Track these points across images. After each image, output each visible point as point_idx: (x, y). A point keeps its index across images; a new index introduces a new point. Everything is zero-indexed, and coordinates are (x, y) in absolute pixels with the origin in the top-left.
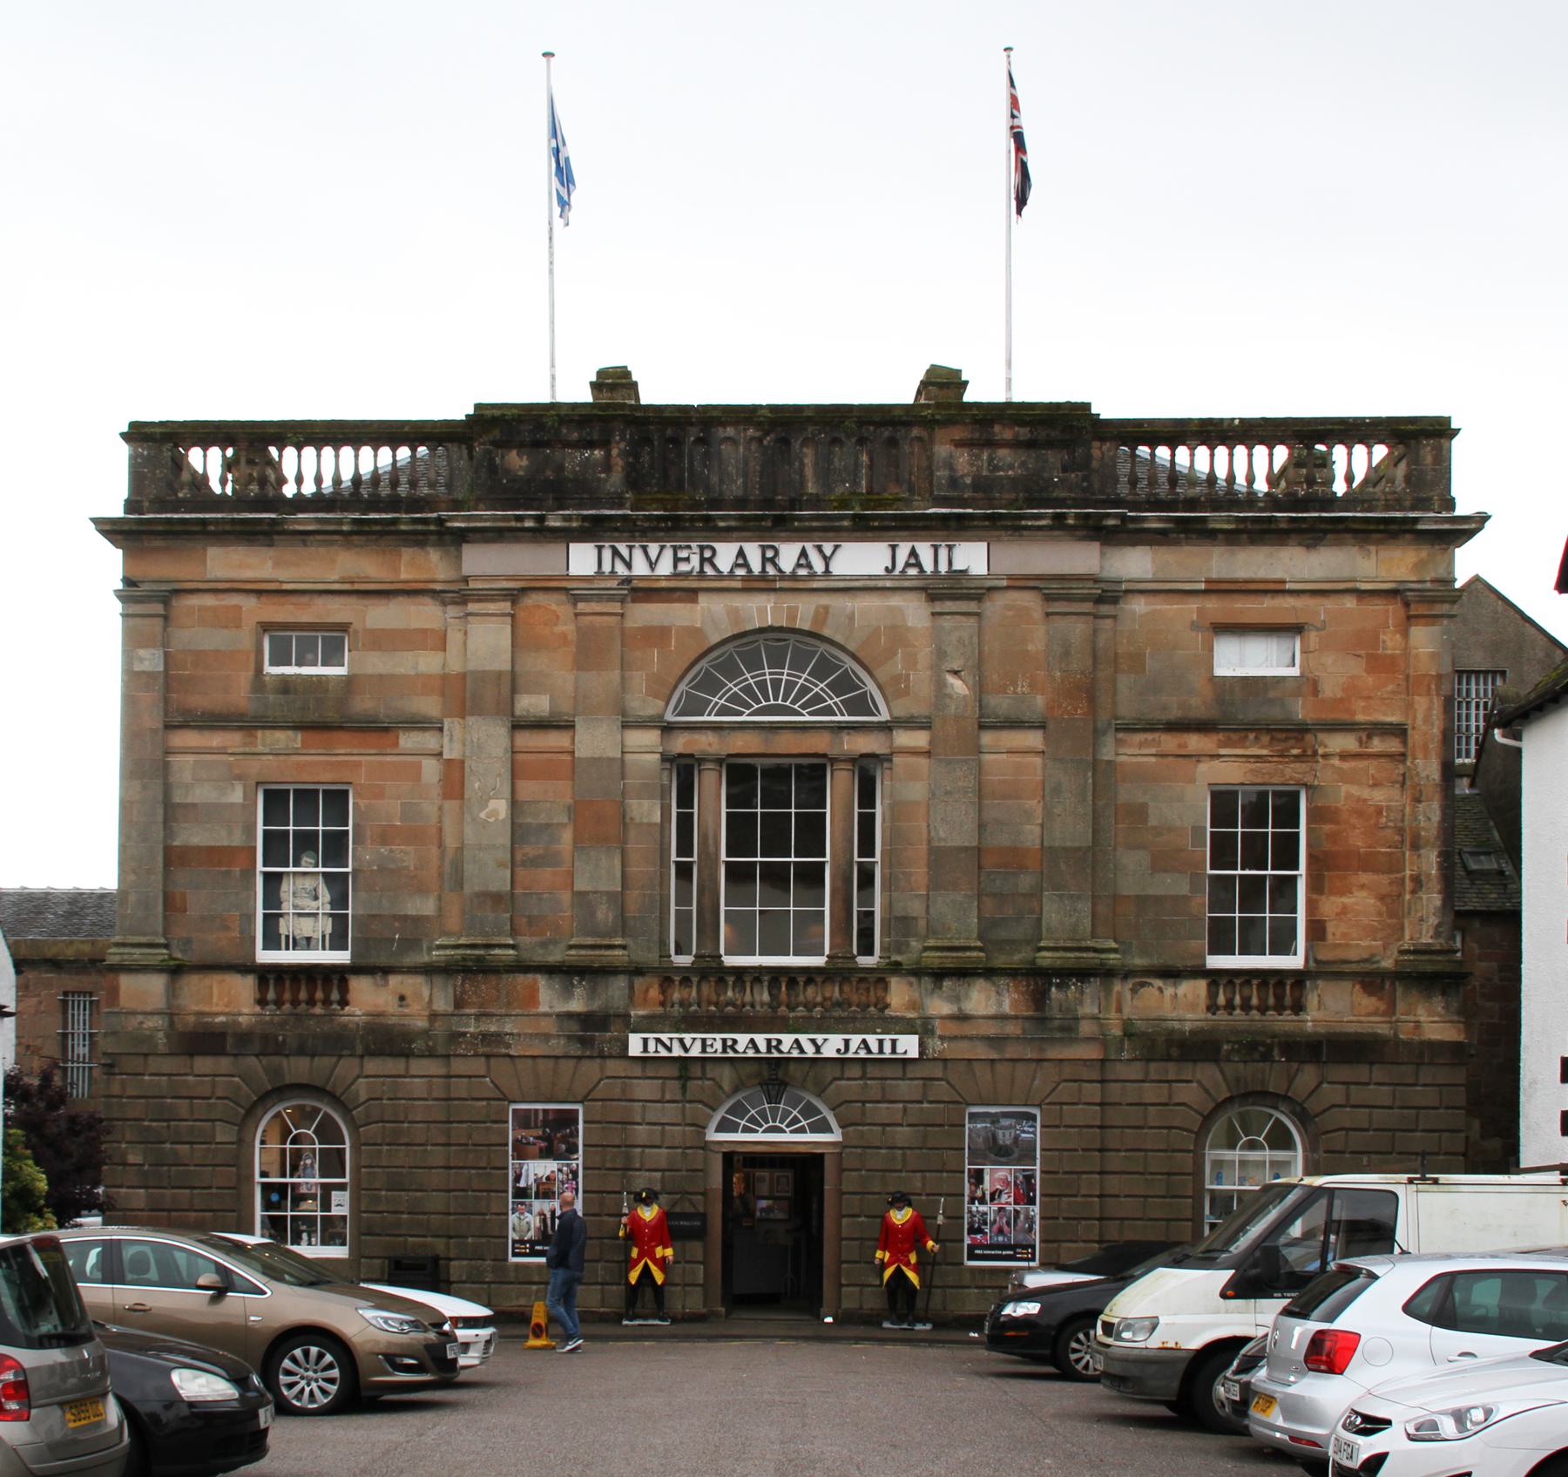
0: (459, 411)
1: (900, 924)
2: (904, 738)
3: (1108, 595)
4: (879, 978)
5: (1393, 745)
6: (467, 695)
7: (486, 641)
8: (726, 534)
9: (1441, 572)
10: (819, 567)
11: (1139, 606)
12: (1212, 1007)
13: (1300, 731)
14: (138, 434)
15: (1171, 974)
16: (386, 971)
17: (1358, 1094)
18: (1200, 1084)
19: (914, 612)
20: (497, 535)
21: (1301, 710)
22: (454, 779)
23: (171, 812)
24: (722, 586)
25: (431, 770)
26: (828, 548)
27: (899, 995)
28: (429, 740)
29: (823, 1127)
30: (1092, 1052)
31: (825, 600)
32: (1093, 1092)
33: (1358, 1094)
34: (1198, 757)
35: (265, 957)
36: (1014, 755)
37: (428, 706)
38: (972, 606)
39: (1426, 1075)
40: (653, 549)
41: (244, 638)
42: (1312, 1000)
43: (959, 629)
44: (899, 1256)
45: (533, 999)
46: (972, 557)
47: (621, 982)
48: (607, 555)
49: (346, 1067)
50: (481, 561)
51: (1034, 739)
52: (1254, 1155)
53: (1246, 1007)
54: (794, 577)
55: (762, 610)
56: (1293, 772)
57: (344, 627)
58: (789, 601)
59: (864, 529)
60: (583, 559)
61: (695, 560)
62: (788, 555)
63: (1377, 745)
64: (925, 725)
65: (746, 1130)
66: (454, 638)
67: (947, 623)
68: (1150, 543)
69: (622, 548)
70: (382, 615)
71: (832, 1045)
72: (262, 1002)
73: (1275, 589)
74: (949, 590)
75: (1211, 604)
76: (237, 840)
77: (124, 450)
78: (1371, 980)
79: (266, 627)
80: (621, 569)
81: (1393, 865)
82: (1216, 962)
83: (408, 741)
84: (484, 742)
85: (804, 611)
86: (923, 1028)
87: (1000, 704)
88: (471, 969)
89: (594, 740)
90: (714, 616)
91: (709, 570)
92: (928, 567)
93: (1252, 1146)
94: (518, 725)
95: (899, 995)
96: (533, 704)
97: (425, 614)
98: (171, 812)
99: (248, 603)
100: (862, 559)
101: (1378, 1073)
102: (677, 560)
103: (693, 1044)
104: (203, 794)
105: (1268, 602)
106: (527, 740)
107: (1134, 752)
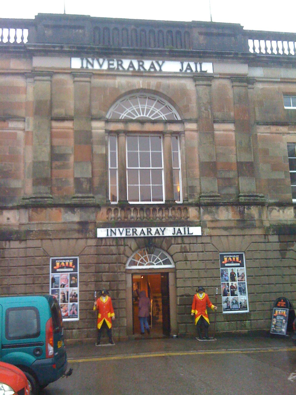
2: (189, 126)
10: (158, 68)
11: (260, 86)
19: (189, 85)
25: (21, 134)
27: (193, 212)
28: (20, 125)
31: (160, 80)
34: (284, 134)
46: (208, 67)
48: (85, 62)
50: (40, 62)
51: (231, 126)
54: (149, 71)
58: (148, 80)
60: (76, 63)
62: (147, 64)
67: (201, 88)
69: (90, 60)
71: (169, 231)
74: (201, 78)
75: (282, 86)
80: (90, 67)
85: (153, 83)
91: (121, 69)
92: (194, 70)
96: (57, 111)
100: (171, 66)
102: (109, 64)
103: (120, 233)
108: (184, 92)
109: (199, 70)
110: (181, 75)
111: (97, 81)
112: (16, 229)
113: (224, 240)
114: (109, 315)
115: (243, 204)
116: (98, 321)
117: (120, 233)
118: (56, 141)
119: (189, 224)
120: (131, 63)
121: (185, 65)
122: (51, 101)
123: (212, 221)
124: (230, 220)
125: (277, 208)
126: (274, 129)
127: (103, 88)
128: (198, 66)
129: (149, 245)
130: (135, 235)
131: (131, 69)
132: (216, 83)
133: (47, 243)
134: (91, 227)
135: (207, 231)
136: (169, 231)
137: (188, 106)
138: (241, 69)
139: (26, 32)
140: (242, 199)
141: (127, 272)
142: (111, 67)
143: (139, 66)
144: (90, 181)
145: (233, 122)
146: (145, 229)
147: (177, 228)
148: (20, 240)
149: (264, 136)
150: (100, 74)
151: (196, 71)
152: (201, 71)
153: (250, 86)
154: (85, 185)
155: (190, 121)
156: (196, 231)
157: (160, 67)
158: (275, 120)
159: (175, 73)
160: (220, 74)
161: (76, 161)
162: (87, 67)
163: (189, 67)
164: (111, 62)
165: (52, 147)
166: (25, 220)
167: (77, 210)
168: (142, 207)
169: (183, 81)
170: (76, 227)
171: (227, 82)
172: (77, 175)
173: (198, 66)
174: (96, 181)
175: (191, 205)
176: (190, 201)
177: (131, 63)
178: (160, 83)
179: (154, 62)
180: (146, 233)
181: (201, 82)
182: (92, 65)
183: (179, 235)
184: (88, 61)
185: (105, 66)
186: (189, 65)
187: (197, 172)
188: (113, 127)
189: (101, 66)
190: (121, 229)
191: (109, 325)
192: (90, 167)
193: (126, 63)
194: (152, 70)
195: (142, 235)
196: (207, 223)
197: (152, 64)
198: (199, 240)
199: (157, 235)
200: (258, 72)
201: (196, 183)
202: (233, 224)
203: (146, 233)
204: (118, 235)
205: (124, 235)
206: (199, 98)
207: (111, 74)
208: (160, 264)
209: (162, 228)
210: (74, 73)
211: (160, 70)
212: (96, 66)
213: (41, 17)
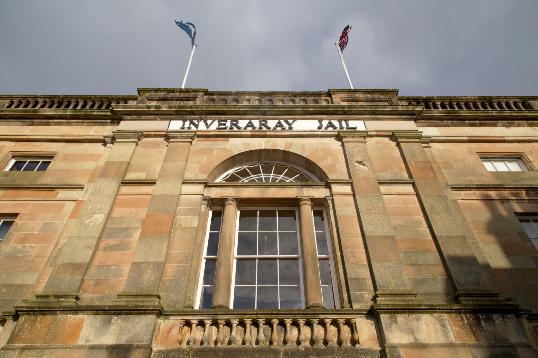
8: (244, 114)
10: (286, 126)
19: (334, 145)
25: (70, 207)
47: (151, 318)
48: (187, 124)
62: (272, 123)
69: (196, 122)
80: (193, 128)
83: (62, 194)
85: (280, 144)
94: (125, 183)
102: (220, 124)
108: (327, 152)
110: (320, 133)
121: (325, 123)
122: (129, 163)
137: (335, 166)
144: (160, 267)
149: (470, 204)
151: (341, 128)
152: (348, 128)
159: (311, 131)
160: (377, 131)
161: (143, 236)
162: (189, 128)
163: (330, 125)
165: (109, 216)
167: (117, 322)
174: (170, 270)
179: (282, 122)
182: (197, 126)
184: (192, 123)
188: (215, 193)
189: (208, 126)
192: (165, 246)
193: (242, 123)
196: (401, 351)
211: (290, 128)
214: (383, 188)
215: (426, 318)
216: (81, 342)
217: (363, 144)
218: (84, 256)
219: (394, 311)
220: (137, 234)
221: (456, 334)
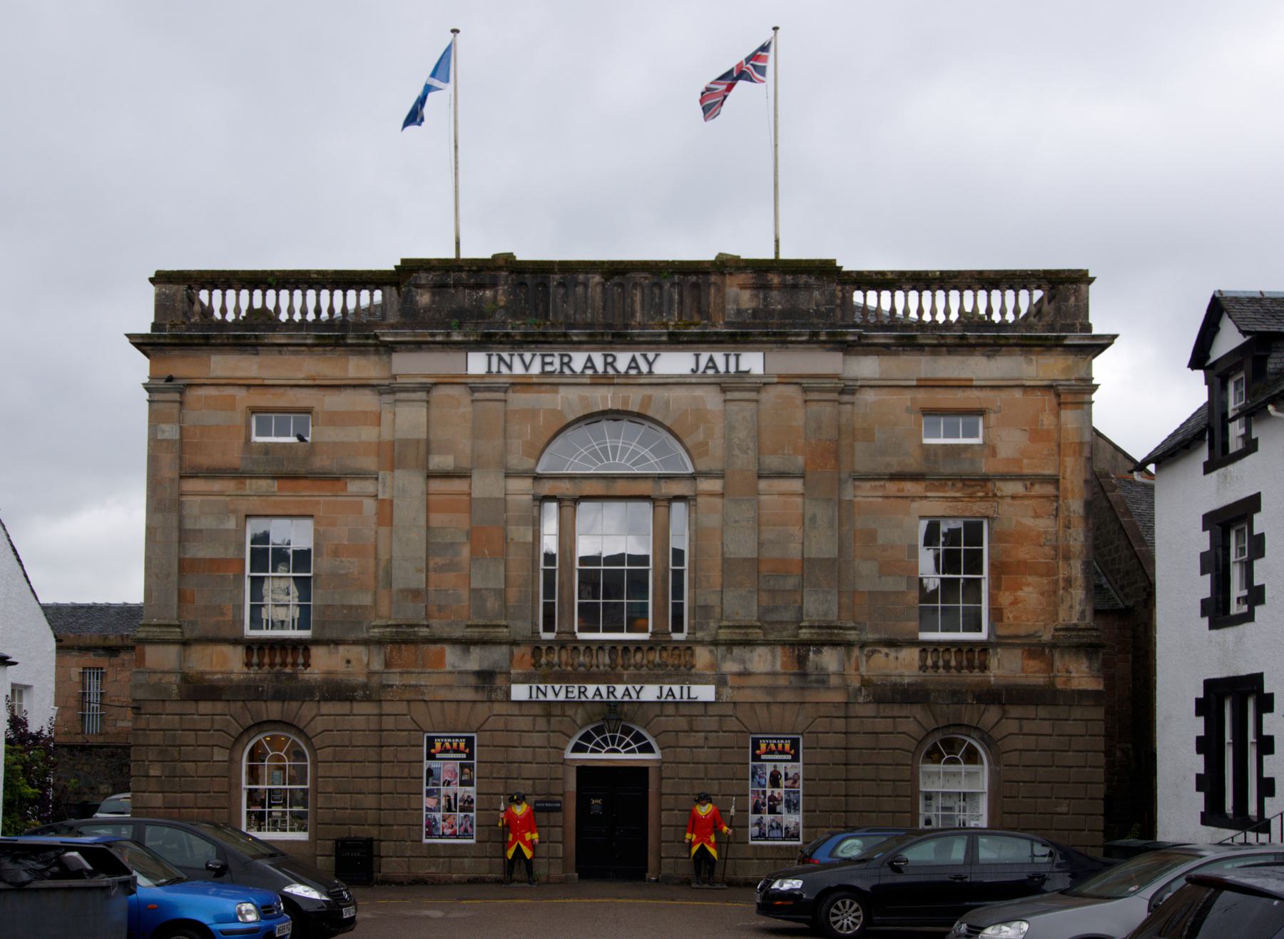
0: (388, 263)
1: (702, 611)
2: (705, 485)
3: (848, 389)
4: (688, 646)
5: (1049, 490)
6: (395, 455)
7: (409, 419)
8: (578, 346)
9: (1082, 374)
10: (644, 368)
11: (869, 396)
12: (923, 667)
13: (985, 479)
14: (161, 278)
15: (892, 644)
16: (337, 643)
17: (1029, 727)
18: (912, 721)
19: (711, 399)
20: (418, 346)
21: (985, 467)
22: (386, 513)
23: (184, 536)
24: (575, 382)
25: (369, 506)
26: (651, 356)
28: (369, 486)
29: (647, 748)
30: (838, 697)
32: (840, 724)
33: (1029, 727)
34: (913, 498)
35: (249, 633)
36: (781, 497)
37: (369, 463)
38: (752, 395)
39: (1077, 713)
40: (527, 356)
41: (239, 418)
42: (993, 662)
43: (742, 412)
44: (703, 837)
45: (441, 659)
46: (753, 362)
47: (505, 649)
48: (495, 360)
49: (308, 710)
50: (409, 365)
51: (796, 485)
52: (952, 768)
53: (947, 666)
54: (626, 375)
55: (605, 398)
56: (978, 508)
57: (308, 411)
59: (676, 341)
60: (477, 363)
61: (557, 361)
62: (623, 360)
63: (1038, 489)
64: (721, 475)
65: (593, 751)
66: (387, 418)
67: (733, 407)
68: (878, 354)
69: (505, 356)
70: (333, 401)
72: (248, 664)
73: (966, 385)
76: (231, 553)
77: (151, 290)
78: (1035, 649)
79: (254, 410)
80: (504, 370)
81: (1050, 571)
82: (925, 636)
83: (353, 486)
84: (407, 487)
85: (633, 399)
86: (721, 682)
87: (773, 462)
88: (401, 639)
89: (485, 485)
90: (569, 401)
92: (722, 368)
93: (954, 761)
94: (431, 476)
95: (702, 656)
96: (440, 461)
97: (367, 401)
98: (184, 536)
99: (240, 393)
100: (675, 363)
101: (1042, 712)
102: (544, 364)
103: (555, 693)
104: (207, 523)
105: (960, 394)
106: (436, 485)
107: (866, 494)
109: (732, 369)
111: (519, 400)
112: (362, 679)
113: (762, 712)
114: (528, 836)
115: (807, 644)
116: (505, 845)
117: (555, 693)
118: (438, 519)
119: (687, 675)
120: (589, 359)
123: (740, 674)
124: (774, 674)
125: (885, 650)
126: (892, 487)
127: (532, 414)
128: (732, 360)
129: (613, 721)
130: (583, 699)
131: (589, 372)
132: (769, 396)
133: (418, 709)
134: (500, 681)
135: (727, 694)
136: (650, 693)
138: (827, 363)
139: (378, 295)
140: (805, 634)
141: (564, 762)
142: (548, 368)
143: (606, 364)
144: (502, 594)
145: (802, 476)
146: (603, 688)
147: (666, 688)
148: (367, 699)
150: (524, 384)
153: (846, 398)
154: (492, 604)
155: (708, 475)
156: (705, 693)
157: (650, 364)
158: (895, 469)
164: (548, 359)
166: (377, 665)
167: (476, 652)
168: (601, 645)
169: (699, 392)
170: (472, 680)
171: (792, 391)
172: (475, 584)
173: (732, 360)
174: (513, 594)
175: (701, 643)
176: (699, 635)
177: (589, 359)
178: (650, 397)
180: (604, 694)
181: (736, 395)
183: (670, 699)
184: (501, 359)
185: (536, 369)
186: (711, 359)
187: (716, 577)
188: (546, 488)
190: (557, 687)
191: (528, 854)
193: (578, 360)
194: (633, 372)
195: (597, 699)
197: (634, 359)
198: (711, 711)
199: (626, 699)
200: (866, 367)
201: (713, 600)
202: (782, 681)
203: (604, 694)
204: (551, 697)
205: (562, 697)
206: (730, 428)
207: (548, 382)
208: (633, 751)
209: (638, 687)
210: (474, 386)
212: (518, 369)
213: (410, 269)
214: (763, 484)
215: (761, 650)
216: (448, 668)
217: (753, 405)
218: (418, 581)
219: (730, 644)
220: (465, 552)
221: (784, 665)
